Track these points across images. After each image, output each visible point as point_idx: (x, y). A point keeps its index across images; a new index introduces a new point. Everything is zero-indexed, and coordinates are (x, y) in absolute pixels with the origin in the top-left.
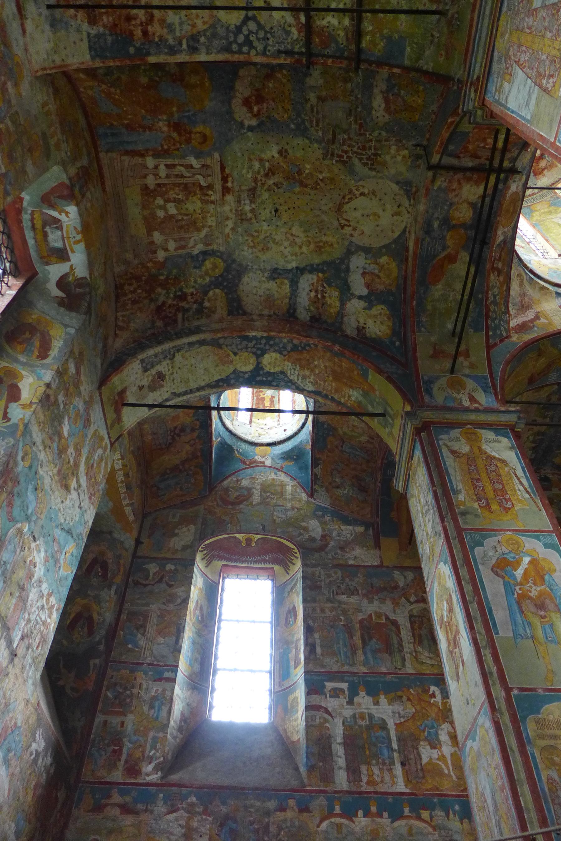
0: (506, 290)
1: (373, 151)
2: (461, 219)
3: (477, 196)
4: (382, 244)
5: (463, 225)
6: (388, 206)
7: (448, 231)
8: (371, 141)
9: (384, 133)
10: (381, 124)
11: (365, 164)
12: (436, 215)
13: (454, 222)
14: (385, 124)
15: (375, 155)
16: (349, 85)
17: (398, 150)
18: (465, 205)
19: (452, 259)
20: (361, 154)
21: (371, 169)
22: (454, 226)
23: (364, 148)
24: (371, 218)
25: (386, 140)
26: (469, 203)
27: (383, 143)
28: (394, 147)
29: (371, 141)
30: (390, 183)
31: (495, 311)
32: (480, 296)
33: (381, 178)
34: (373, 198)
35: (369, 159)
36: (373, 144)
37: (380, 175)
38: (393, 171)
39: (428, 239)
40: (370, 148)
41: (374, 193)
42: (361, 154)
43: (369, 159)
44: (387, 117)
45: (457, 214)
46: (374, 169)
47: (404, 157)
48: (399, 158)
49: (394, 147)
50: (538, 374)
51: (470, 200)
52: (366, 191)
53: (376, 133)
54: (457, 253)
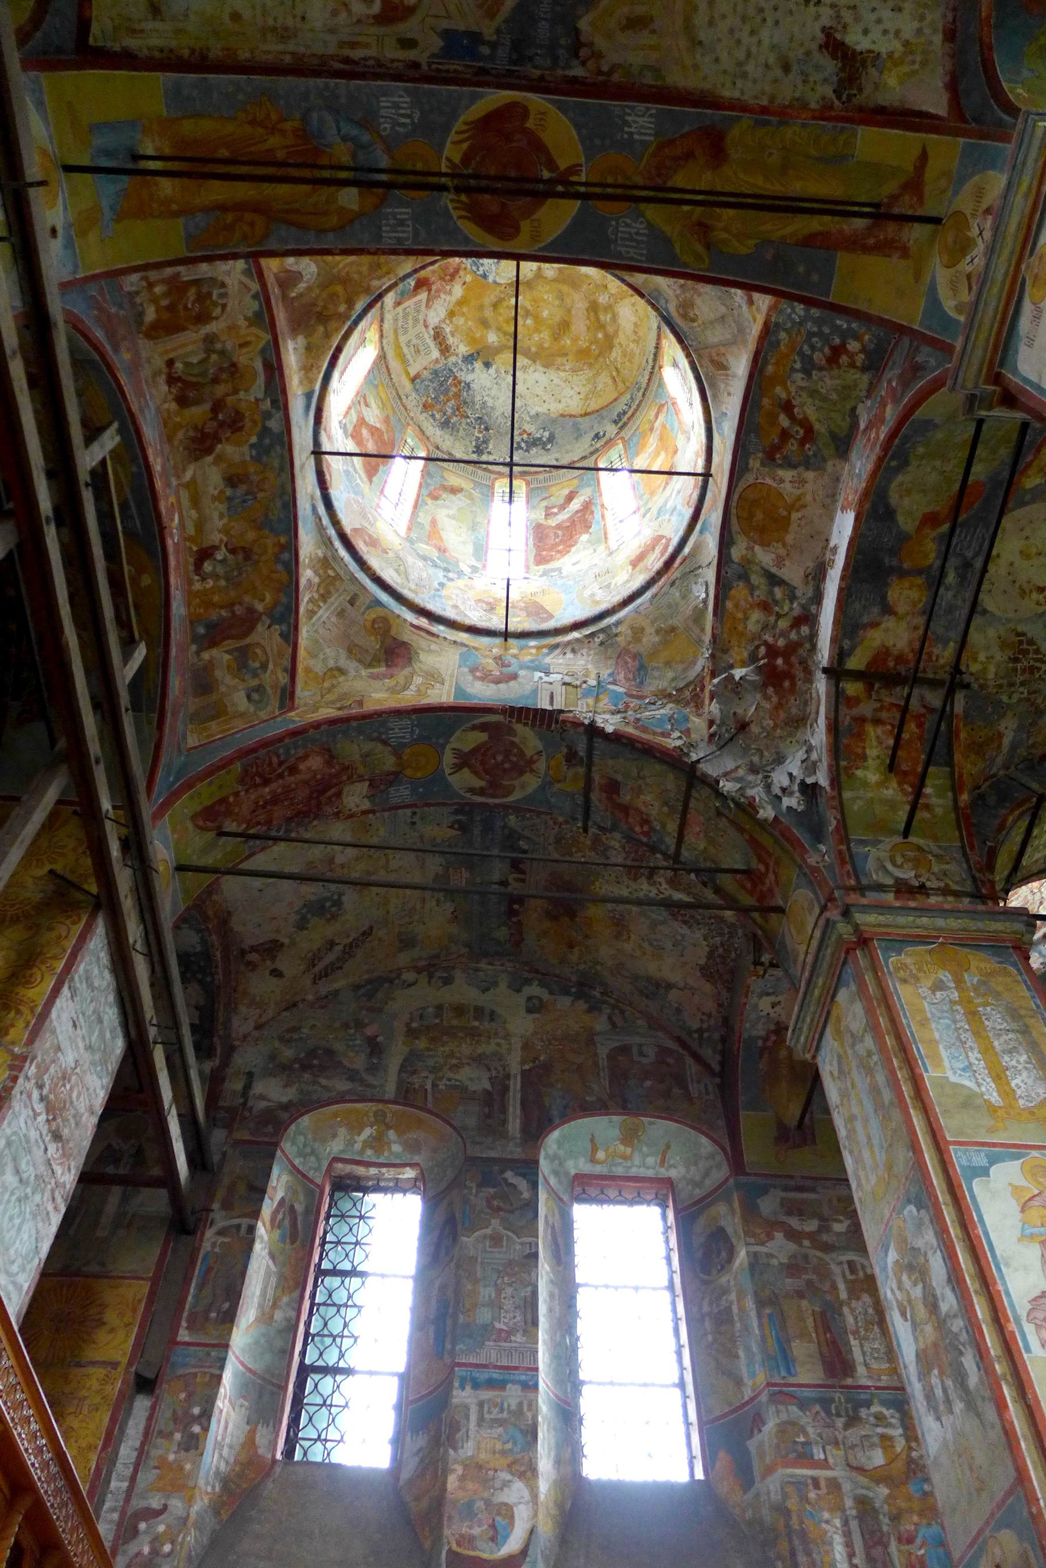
0: (766, 362)
1: (1019, 665)
2: (907, 584)
3: (883, 626)
4: (1027, 508)
5: (902, 574)
6: (1003, 571)
7: (931, 566)
8: (1022, 684)
9: (1005, 698)
10: (1010, 714)
11: (1031, 642)
12: (950, 594)
13: (919, 581)
14: (1003, 716)
15: (1016, 660)
16: (1030, 742)
17: (985, 670)
18: (901, 609)
19: (931, 520)
20: (1036, 660)
21: (1023, 634)
22: (920, 572)
23: (1032, 670)
24: (1034, 551)
25: (1000, 686)
26: (895, 614)
27: (1005, 682)
28: (991, 675)
29: (1022, 684)
30: (998, 613)
31: (813, 348)
32: (894, 463)
33: (1009, 620)
34: (1025, 586)
35: (1025, 652)
36: (1019, 679)
37: (1012, 625)
38: (991, 633)
39: (969, 554)
40: (1024, 671)
41: (1023, 593)
42: (1036, 660)
43: (1025, 652)
44: (1002, 729)
45: (914, 594)
46: (1018, 634)
47: (975, 660)
48: (982, 657)
49: (991, 675)
50: (689, 155)
51: (893, 619)
52: (1035, 596)
53: (1016, 697)
54: (919, 529)
